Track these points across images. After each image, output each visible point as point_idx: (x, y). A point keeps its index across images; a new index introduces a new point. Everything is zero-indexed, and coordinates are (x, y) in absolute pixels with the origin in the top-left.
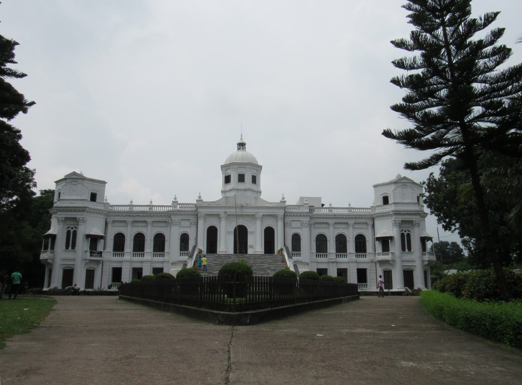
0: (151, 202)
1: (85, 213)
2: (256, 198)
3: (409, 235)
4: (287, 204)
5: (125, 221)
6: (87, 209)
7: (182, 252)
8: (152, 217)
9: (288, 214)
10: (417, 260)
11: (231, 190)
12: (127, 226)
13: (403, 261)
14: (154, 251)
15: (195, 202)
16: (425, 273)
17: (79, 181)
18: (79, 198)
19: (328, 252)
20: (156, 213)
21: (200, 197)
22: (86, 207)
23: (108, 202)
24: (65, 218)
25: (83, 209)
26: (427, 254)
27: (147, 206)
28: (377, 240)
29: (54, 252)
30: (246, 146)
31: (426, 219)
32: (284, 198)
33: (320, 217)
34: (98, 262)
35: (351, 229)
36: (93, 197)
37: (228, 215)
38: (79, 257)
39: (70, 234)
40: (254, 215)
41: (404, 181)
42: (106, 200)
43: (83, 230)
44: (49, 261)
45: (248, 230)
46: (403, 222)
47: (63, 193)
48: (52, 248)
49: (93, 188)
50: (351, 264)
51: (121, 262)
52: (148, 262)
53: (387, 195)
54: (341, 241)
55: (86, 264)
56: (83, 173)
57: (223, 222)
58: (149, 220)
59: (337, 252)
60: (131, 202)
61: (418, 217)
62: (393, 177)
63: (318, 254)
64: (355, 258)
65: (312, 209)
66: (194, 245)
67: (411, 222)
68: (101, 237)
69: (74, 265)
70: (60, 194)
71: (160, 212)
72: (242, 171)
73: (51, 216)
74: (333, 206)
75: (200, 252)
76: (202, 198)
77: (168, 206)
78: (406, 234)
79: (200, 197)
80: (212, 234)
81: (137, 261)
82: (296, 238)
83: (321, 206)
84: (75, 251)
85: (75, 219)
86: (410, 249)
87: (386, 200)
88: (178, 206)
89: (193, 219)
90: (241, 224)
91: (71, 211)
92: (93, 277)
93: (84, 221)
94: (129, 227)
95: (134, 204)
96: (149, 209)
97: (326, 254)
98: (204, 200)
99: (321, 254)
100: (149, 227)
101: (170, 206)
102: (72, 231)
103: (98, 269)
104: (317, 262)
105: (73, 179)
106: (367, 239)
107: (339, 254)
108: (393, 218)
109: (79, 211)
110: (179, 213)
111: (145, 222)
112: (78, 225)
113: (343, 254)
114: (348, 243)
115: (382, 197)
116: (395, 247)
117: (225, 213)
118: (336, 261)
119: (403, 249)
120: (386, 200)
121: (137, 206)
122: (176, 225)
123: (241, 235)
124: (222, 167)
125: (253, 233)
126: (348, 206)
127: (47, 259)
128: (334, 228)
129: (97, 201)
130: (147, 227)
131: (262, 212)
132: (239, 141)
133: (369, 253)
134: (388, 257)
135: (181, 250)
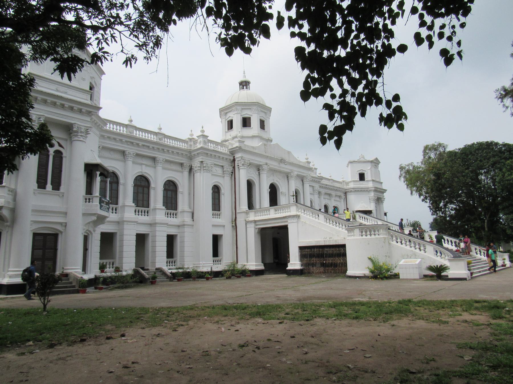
11: (253, 137)
35: (333, 200)
39: (48, 156)
53: (364, 172)
58: (160, 156)
69: (65, 225)
71: (173, 148)
87: (362, 177)
90: (275, 182)
94: (130, 163)
95: (134, 123)
100: (159, 168)
108: (372, 194)
110: (214, 154)
120: (362, 177)
122: (208, 171)
131: (296, 171)
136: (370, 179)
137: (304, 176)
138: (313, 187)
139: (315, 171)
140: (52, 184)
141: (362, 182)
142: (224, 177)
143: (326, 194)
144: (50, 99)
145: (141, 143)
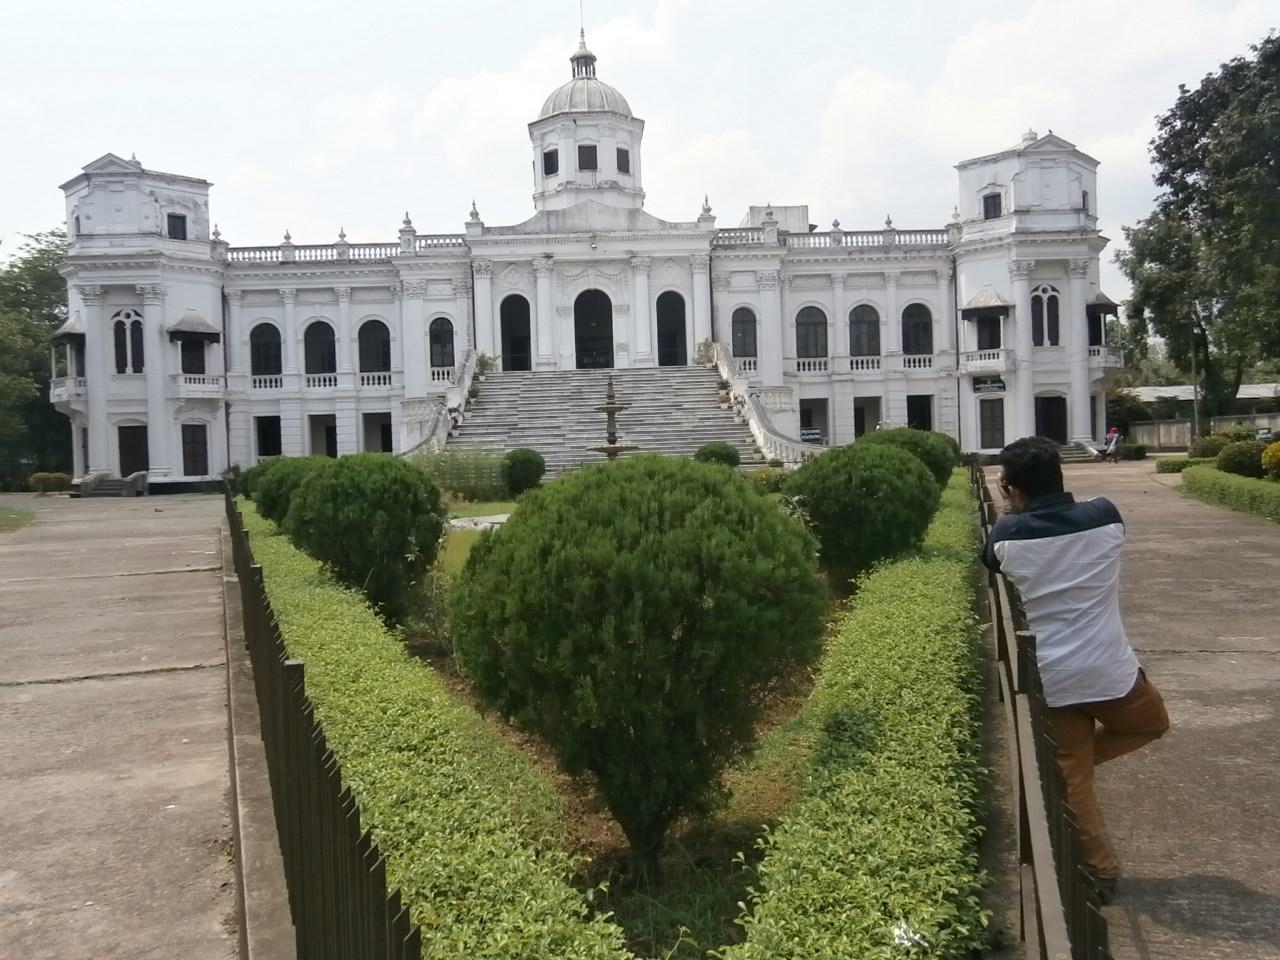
0: (342, 236)
1: (157, 272)
2: (634, 213)
3: (1053, 301)
4: (718, 225)
5: (277, 291)
6: (163, 260)
7: (436, 369)
8: (348, 277)
10: (1074, 370)
12: (282, 303)
13: (1034, 373)
14: (365, 366)
15: (463, 230)
16: (1093, 400)
17: (128, 180)
18: (134, 229)
19: (830, 355)
20: (357, 262)
21: (475, 214)
22: (161, 254)
23: (221, 238)
24: (102, 286)
25: (150, 261)
26: (1102, 350)
27: (332, 246)
28: (964, 318)
29: (85, 382)
30: (596, 64)
31: (1102, 255)
32: (709, 210)
33: (808, 261)
34: (211, 404)
35: (891, 288)
36: (177, 227)
37: (555, 263)
38: (160, 393)
39: (124, 331)
40: (627, 262)
41: (1049, 148)
42: (216, 234)
43: (156, 320)
44: (75, 406)
45: (613, 302)
46: (1039, 263)
47: (88, 218)
48: (81, 372)
49: (176, 200)
50: (892, 386)
51: (277, 401)
52: (348, 396)
53: (998, 190)
54: (865, 322)
55: (179, 411)
56: (138, 159)
57: (543, 283)
58: (341, 285)
59: (852, 354)
60: (288, 237)
61: (1084, 248)
62: (1016, 142)
63: (802, 360)
64: (902, 368)
65: (783, 237)
66: (466, 348)
67: (1064, 265)
68: (214, 338)
69: (146, 413)
70: (77, 219)
71: (369, 262)
72: (587, 137)
73: (63, 281)
74: (843, 227)
75: (483, 364)
76: (482, 218)
77: (391, 245)
78: (1045, 297)
79: (475, 214)
80: (515, 315)
81: (319, 398)
82: (745, 321)
83: (807, 231)
84: (145, 379)
85: (131, 289)
86: (1055, 341)
87: (992, 206)
88: (418, 244)
89: (458, 275)
90: (592, 287)
91: (116, 267)
92: (205, 444)
93: (156, 293)
94: (289, 307)
95: (294, 241)
96: (339, 254)
97: (823, 360)
99: (812, 360)
100: (344, 305)
101: (396, 245)
102: (128, 323)
103: (212, 421)
104: (801, 384)
105: (107, 175)
106: (935, 316)
107: (860, 358)
108: (1014, 254)
109: (139, 266)
110: (420, 261)
111: (331, 290)
112: (143, 305)
113: (870, 358)
114: (883, 330)
115: (980, 196)
116: (1017, 332)
117: (548, 257)
118: (850, 377)
119: (1038, 340)
121: (305, 247)
122: (414, 295)
123: (593, 319)
124: (531, 125)
126: (883, 227)
127: (68, 403)
128: (846, 288)
129: (189, 236)
130: (336, 302)
132: (575, 50)
133: (939, 355)
134: (996, 364)
135: (432, 366)
136: (1012, 210)
138: (754, 271)
140: (134, 365)
141: (989, 224)
142: (455, 299)
144: (98, 262)
145: (299, 272)
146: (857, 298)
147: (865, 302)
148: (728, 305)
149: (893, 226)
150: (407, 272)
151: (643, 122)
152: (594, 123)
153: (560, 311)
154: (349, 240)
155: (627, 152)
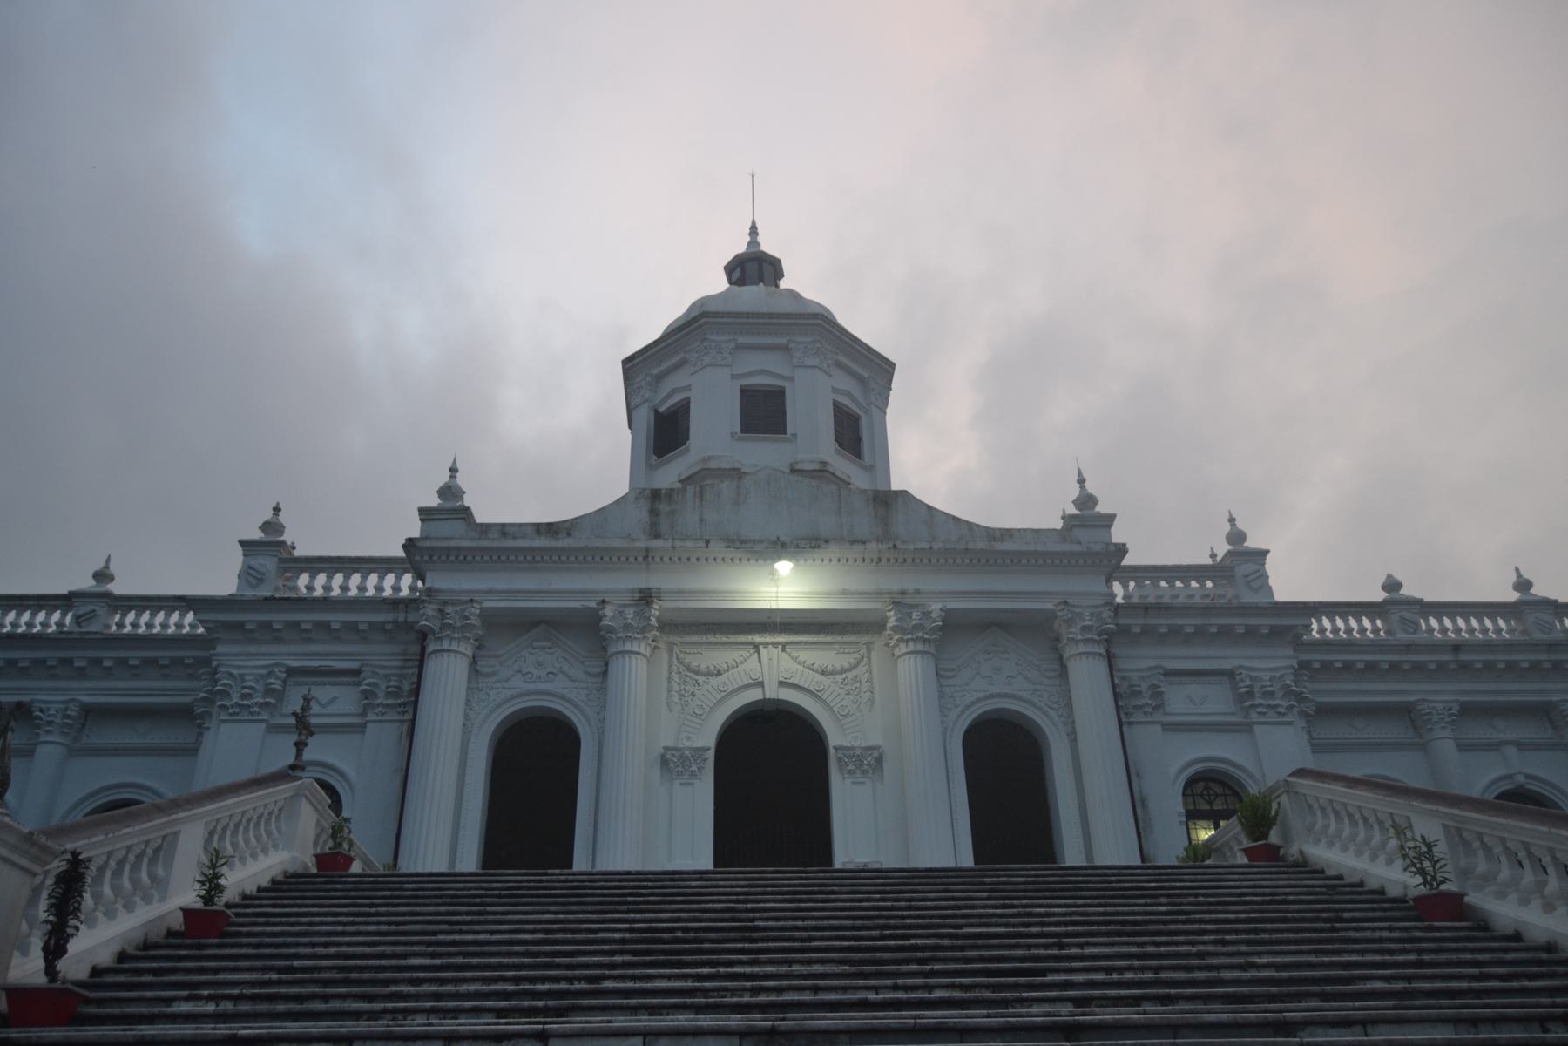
0: (103, 576)
8: (81, 674)
9: (1136, 623)
21: (450, 491)
27: (65, 601)
32: (1086, 500)
33: (1348, 667)
72: (763, 368)
79: (450, 491)
90: (773, 692)
96: (78, 620)
98: (480, 518)
117: (646, 597)
124: (632, 365)
125: (870, 762)
126: (1513, 596)
137: (1050, 617)
138: (1230, 674)
139: (1243, 569)
142: (364, 726)
143: (1469, 711)
146: (1504, 772)
147: (1521, 779)
148: (1172, 760)
149: (1539, 591)
150: (235, 649)
151: (892, 365)
152: (782, 340)
153: (672, 763)
154: (117, 588)
155: (855, 420)
